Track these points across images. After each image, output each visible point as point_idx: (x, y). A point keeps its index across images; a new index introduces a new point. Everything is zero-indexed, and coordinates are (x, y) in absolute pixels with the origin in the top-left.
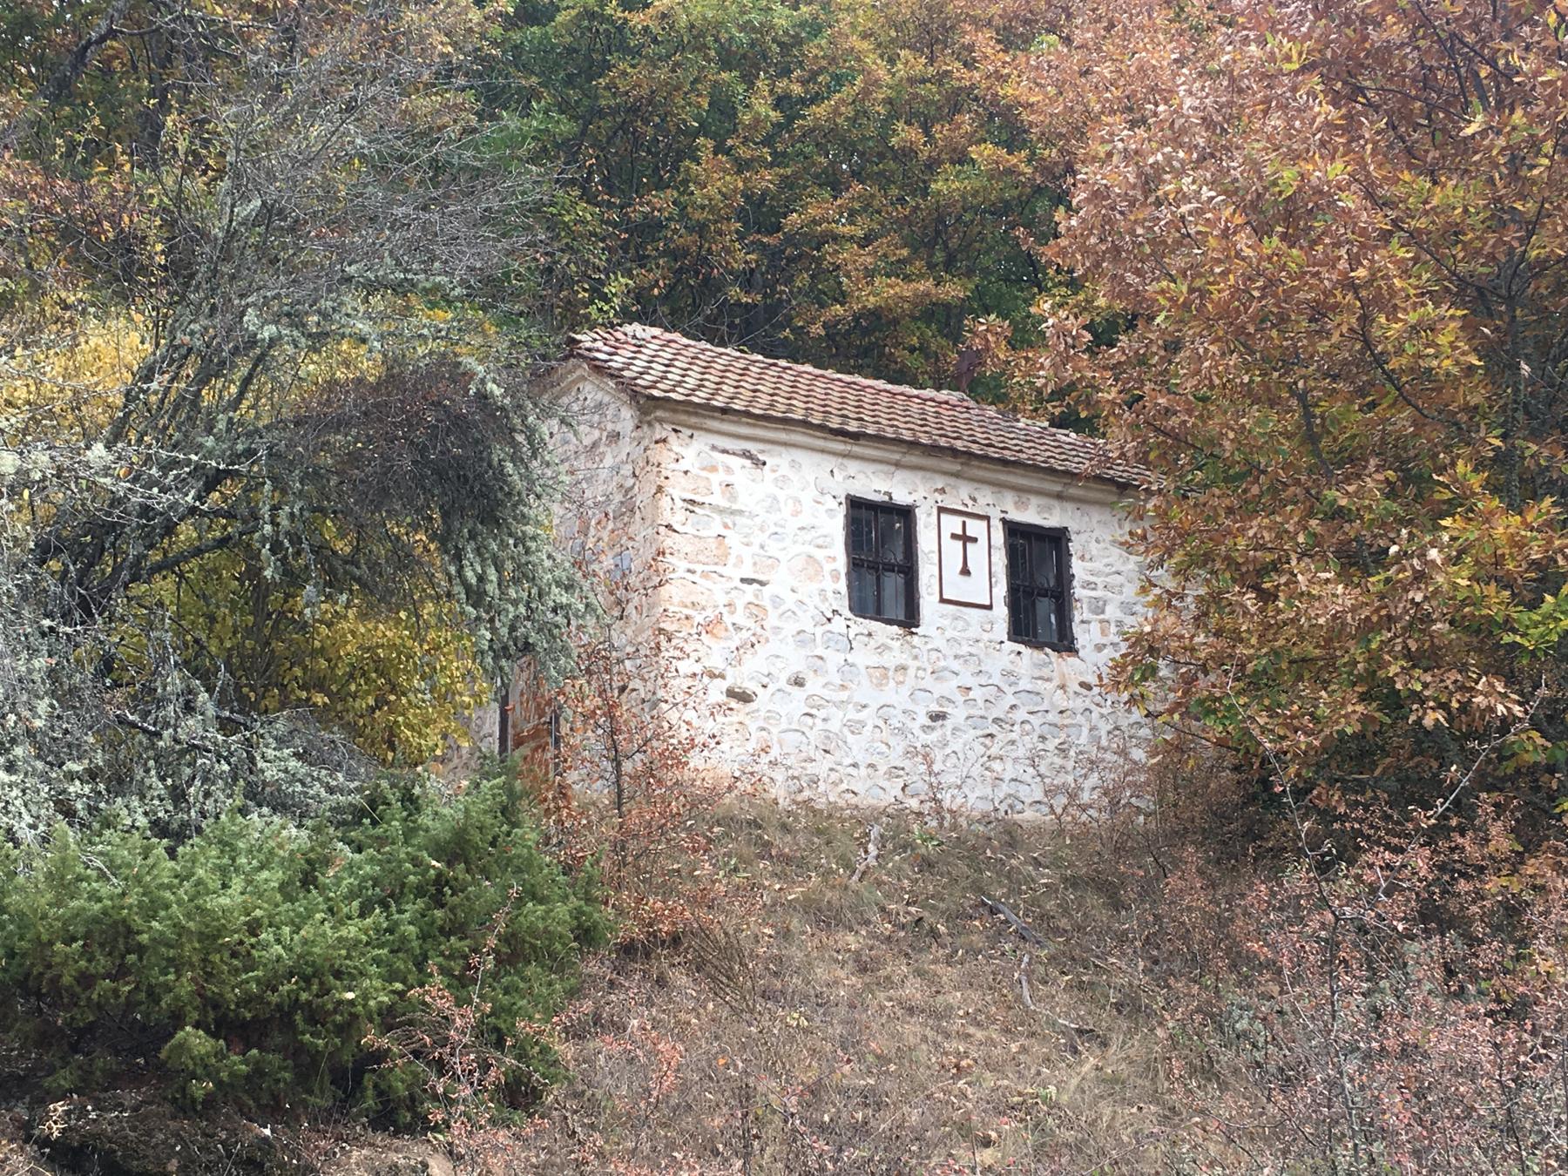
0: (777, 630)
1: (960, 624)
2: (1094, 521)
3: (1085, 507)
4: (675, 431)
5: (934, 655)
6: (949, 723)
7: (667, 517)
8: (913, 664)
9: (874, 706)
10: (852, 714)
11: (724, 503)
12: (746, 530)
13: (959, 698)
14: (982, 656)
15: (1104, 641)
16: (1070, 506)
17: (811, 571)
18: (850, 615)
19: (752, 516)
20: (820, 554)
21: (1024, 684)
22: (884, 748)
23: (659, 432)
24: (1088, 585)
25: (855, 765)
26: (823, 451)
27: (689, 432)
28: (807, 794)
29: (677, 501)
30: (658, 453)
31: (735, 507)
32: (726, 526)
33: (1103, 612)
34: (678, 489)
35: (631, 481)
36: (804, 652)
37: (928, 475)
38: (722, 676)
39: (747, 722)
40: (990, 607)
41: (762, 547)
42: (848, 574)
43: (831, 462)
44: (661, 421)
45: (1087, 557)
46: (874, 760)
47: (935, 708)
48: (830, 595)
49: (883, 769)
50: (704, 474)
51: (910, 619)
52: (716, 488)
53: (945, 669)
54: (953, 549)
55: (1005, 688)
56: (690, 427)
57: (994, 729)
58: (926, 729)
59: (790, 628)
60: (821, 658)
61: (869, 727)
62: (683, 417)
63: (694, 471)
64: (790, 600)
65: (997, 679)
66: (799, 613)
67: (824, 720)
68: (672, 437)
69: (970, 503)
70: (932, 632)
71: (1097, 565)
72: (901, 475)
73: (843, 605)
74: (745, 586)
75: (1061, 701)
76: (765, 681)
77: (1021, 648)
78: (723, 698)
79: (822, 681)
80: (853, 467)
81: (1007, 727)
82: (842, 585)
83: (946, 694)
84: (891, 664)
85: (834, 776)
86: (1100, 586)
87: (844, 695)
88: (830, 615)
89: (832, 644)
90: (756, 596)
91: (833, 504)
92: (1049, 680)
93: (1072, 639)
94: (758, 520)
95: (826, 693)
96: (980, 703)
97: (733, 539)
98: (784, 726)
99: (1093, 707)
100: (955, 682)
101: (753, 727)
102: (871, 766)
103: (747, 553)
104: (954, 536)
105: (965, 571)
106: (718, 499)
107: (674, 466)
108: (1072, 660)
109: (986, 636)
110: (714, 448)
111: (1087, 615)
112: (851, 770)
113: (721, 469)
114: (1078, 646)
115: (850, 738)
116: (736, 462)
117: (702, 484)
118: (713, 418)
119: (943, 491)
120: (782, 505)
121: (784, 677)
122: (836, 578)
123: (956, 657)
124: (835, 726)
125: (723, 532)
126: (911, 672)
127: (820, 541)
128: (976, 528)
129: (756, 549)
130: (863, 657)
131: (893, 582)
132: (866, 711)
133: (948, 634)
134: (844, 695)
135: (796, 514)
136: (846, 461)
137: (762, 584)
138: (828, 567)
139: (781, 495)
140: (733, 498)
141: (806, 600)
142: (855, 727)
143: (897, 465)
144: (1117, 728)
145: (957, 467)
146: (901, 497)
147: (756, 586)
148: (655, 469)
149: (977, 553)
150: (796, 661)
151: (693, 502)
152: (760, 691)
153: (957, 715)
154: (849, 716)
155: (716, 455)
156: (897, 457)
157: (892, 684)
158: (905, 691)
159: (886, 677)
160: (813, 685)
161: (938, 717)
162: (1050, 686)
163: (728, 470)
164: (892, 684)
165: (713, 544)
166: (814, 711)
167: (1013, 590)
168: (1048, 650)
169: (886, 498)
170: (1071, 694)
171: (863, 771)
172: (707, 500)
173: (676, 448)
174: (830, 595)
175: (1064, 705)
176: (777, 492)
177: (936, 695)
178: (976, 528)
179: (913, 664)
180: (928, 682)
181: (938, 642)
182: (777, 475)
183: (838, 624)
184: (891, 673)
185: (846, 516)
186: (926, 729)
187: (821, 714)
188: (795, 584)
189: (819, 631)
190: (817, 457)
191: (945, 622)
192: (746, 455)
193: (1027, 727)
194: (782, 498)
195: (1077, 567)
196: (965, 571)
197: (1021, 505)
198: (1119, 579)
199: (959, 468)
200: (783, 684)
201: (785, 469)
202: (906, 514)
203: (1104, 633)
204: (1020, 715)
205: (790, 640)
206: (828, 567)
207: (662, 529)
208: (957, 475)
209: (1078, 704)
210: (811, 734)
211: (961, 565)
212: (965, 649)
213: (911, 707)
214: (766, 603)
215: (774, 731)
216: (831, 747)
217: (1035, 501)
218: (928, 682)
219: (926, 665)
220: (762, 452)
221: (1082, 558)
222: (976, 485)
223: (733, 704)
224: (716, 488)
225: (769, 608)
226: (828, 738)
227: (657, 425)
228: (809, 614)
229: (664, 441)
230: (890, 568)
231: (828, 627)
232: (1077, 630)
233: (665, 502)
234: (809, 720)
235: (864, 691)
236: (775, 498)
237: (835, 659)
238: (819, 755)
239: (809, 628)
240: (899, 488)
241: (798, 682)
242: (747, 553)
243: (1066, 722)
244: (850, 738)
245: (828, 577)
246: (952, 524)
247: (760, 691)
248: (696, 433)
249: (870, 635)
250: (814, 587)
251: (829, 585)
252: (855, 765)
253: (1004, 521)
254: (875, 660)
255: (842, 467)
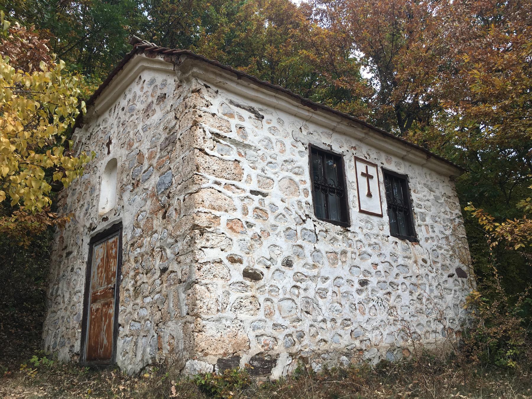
0: (274, 227)
1: (369, 226)
2: (417, 173)
3: (413, 165)
4: (207, 87)
5: (359, 244)
6: (370, 287)
7: (200, 143)
8: (349, 250)
9: (332, 278)
10: (321, 285)
11: (238, 139)
12: (253, 159)
13: (373, 271)
14: (381, 245)
15: (428, 236)
16: (407, 164)
17: (292, 188)
18: (315, 219)
19: (257, 150)
20: (297, 178)
21: (401, 261)
22: (338, 307)
23: (194, 84)
24: (419, 206)
25: (324, 321)
26: (295, 116)
27: (216, 89)
28: (297, 347)
29: (207, 132)
30: (193, 99)
31: (246, 142)
32: (240, 154)
33: (425, 221)
34: (209, 125)
35: (174, 122)
36: (291, 243)
37: (348, 138)
38: (240, 261)
39: (258, 295)
40: (381, 216)
41: (263, 171)
42: (312, 192)
43: (300, 123)
44: (196, 77)
45: (416, 191)
46: (335, 315)
47: (362, 277)
48: (304, 204)
49: (339, 321)
50: (226, 118)
51: (344, 221)
52: (233, 129)
53: (365, 252)
54: (363, 181)
55: (393, 264)
56: (216, 86)
57: (390, 289)
58: (359, 291)
59: (282, 227)
60: (301, 246)
61: (330, 293)
62: (212, 76)
63: (219, 115)
64: (281, 206)
65: (388, 259)
66: (287, 216)
67: (305, 290)
68: (204, 90)
69: (368, 157)
70: (357, 230)
71: (420, 196)
72: (335, 136)
73: (311, 212)
74: (253, 196)
75: (415, 270)
76: (269, 263)
77: (397, 240)
78: (241, 278)
79: (303, 262)
80: (312, 128)
81: (395, 287)
82: (310, 199)
83: (367, 269)
84: (339, 251)
85: (313, 330)
86: (423, 207)
87: (315, 272)
88: (304, 218)
89: (306, 237)
90: (261, 204)
91: (303, 149)
92: (410, 258)
93: (416, 235)
94: (260, 153)
95: (304, 270)
96: (383, 273)
97: (245, 164)
98: (281, 296)
99: (429, 273)
100: (370, 261)
101: (261, 300)
102: (333, 320)
103: (253, 173)
104: (363, 174)
105: (369, 195)
106: (234, 135)
107: (205, 108)
108: (417, 246)
109: (381, 233)
110: (231, 102)
111: (420, 222)
112: (322, 325)
113: (236, 117)
114: (419, 239)
115: (321, 302)
116: (246, 114)
117: (224, 124)
118: (231, 80)
119: (355, 148)
120: (274, 145)
121: (280, 260)
122: (307, 195)
123: (370, 245)
124: (311, 293)
125: (238, 158)
126: (349, 254)
127: (296, 170)
128: (372, 171)
129: (259, 171)
130: (323, 246)
131: (333, 198)
132: (328, 282)
133: (365, 231)
134: (315, 272)
135: (283, 151)
136: (307, 124)
137: (264, 195)
138: (302, 187)
139: (273, 138)
140: (245, 136)
141: (291, 208)
142: (322, 293)
143: (334, 130)
144: (439, 285)
145: (361, 135)
146: (337, 149)
147: (260, 196)
148: (192, 110)
149: (374, 183)
150: (286, 248)
151: (218, 135)
152: (265, 271)
153: (373, 281)
154: (318, 287)
155: (232, 107)
156: (334, 124)
157: (340, 263)
158: (347, 267)
159: (336, 258)
160: (297, 266)
161: (364, 283)
162: (411, 262)
163: (241, 118)
164: (340, 263)
165: (232, 166)
166: (298, 284)
167: (389, 207)
168: (408, 241)
169: (329, 148)
170: (420, 266)
171: (329, 324)
172: (228, 135)
173: (207, 97)
174: (304, 204)
175: (418, 272)
176: (270, 136)
177: (362, 270)
178: (372, 171)
179: (349, 250)
180: (357, 262)
181: (360, 237)
182: (270, 125)
183: (309, 225)
184: (339, 256)
185: (309, 156)
186: (359, 291)
187: (303, 285)
188: (284, 197)
189: (299, 228)
190: (292, 119)
191: (363, 224)
192: (251, 110)
193: (404, 286)
194: (274, 141)
195: (414, 196)
196: (369, 195)
197: (389, 161)
198: (429, 204)
199: (363, 135)
200: (279, 265)
201: (274, 123)
202: (338, 159)
203: (428, 232)
204: (401, 279)
205: (282, 234)
206: (302, 187)
207: (197, 151)
208: (360, 140)
209: (422, 271)
210: (298, 301)
211: (366, 194)
212: (373, 241)
213: (350, 278)
214: (267, 208)
215: (275, 300)
216: (310, 309)
217: (394, 159)
218: (357, 262)
219: (356, 250)
220: (261, 110)
221: (414, 191)
222: (369, 148)
223: (248, 282)
224: (233, 129)
225: (269, 212)
226: (308, 302)
227: (194, 81)
228: (293, 217)
229: (198, 91)
230: (332, 191)
231: (304, 226)
232: (417, 229)
233: (199, 132)
234: (296, 291)
235: (326, 270)
236: (270, 140)
237: (309, 247)
238: (304, 316)
239: (293, 227)
240: (337, 145)
241: (288, 263)
242: (253, 173)
243: (420, 282)
244: (321, 302)
245: (302, 193)
246: (361, 168)
247: (265, 271)
248: (220, 91)
249: (326, 231)
250: (295, 199)
251: (303, 199)
252: (324, 321)
253: (382, 167)
254: (330, 248)
255: (306, 128)
